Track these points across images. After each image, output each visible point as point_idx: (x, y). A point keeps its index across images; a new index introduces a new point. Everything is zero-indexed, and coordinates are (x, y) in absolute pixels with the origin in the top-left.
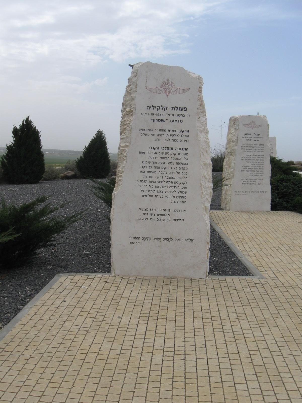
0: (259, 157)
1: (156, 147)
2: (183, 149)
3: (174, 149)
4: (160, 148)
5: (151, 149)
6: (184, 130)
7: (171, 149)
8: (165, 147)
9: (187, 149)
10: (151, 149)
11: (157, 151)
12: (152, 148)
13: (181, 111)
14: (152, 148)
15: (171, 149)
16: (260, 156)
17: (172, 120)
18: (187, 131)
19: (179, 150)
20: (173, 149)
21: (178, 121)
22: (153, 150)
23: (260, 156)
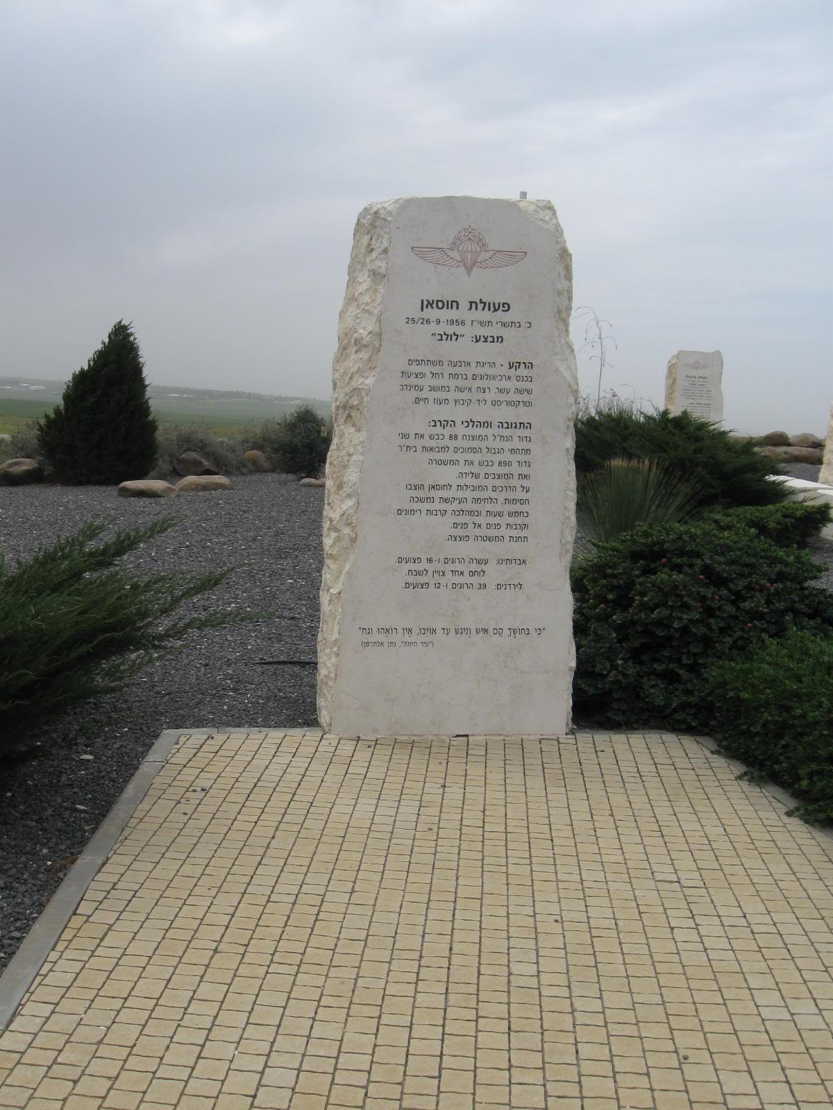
18: (527, 365)
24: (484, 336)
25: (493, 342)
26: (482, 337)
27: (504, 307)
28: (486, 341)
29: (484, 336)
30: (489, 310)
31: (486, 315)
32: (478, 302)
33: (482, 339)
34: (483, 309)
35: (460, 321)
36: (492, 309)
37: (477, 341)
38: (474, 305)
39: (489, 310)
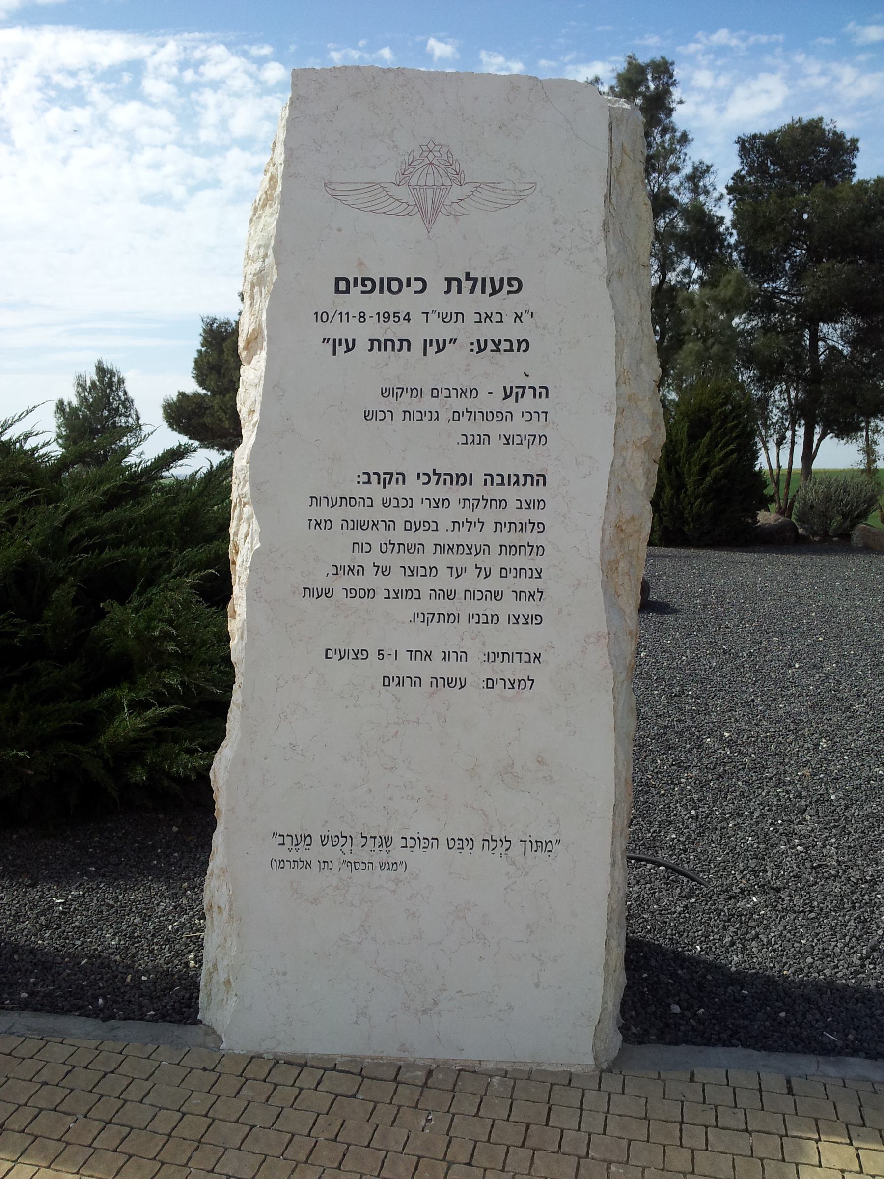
0: (497, 492)
1: (391, 474)
2: (522, 481)
3: (478, 479)
4: (411, 477)
5: (369, 482)
6: (524, 388)
7: (462, 479)
8: (435, 474)
9: (541, 478)
10: (369, 482)
11: (393, 490)
12: (374, 478)
13: (490, 295)
14: (374, 478)
15: (462, 479)
16: (505, 480)
17: (478, 341)
19: (503, 484)
20: (471, 484)
21: (507, 346)
22: (375, 491)
23: (505, 480)
24: (493, 341)
25: (511, 350)
26: (490, 344)
27: (510, 285)
28: (498, 350)
29: (493, 341)
30: (483, 292)
31: (486, 303)
32: (463, 278)
33: (491, 346)
34: (472, 292)
35: (402, 316)
36: (489, 290)
37: (480, 350)
38: (454, 284)
39: (483, 292)
